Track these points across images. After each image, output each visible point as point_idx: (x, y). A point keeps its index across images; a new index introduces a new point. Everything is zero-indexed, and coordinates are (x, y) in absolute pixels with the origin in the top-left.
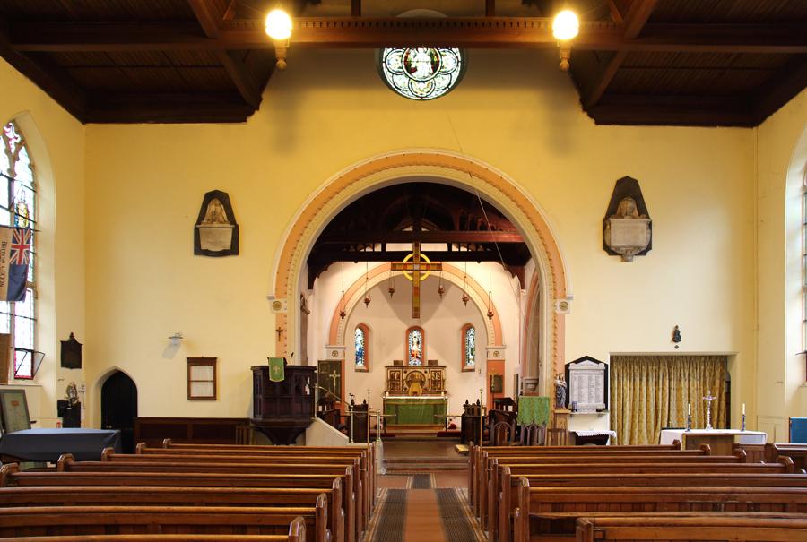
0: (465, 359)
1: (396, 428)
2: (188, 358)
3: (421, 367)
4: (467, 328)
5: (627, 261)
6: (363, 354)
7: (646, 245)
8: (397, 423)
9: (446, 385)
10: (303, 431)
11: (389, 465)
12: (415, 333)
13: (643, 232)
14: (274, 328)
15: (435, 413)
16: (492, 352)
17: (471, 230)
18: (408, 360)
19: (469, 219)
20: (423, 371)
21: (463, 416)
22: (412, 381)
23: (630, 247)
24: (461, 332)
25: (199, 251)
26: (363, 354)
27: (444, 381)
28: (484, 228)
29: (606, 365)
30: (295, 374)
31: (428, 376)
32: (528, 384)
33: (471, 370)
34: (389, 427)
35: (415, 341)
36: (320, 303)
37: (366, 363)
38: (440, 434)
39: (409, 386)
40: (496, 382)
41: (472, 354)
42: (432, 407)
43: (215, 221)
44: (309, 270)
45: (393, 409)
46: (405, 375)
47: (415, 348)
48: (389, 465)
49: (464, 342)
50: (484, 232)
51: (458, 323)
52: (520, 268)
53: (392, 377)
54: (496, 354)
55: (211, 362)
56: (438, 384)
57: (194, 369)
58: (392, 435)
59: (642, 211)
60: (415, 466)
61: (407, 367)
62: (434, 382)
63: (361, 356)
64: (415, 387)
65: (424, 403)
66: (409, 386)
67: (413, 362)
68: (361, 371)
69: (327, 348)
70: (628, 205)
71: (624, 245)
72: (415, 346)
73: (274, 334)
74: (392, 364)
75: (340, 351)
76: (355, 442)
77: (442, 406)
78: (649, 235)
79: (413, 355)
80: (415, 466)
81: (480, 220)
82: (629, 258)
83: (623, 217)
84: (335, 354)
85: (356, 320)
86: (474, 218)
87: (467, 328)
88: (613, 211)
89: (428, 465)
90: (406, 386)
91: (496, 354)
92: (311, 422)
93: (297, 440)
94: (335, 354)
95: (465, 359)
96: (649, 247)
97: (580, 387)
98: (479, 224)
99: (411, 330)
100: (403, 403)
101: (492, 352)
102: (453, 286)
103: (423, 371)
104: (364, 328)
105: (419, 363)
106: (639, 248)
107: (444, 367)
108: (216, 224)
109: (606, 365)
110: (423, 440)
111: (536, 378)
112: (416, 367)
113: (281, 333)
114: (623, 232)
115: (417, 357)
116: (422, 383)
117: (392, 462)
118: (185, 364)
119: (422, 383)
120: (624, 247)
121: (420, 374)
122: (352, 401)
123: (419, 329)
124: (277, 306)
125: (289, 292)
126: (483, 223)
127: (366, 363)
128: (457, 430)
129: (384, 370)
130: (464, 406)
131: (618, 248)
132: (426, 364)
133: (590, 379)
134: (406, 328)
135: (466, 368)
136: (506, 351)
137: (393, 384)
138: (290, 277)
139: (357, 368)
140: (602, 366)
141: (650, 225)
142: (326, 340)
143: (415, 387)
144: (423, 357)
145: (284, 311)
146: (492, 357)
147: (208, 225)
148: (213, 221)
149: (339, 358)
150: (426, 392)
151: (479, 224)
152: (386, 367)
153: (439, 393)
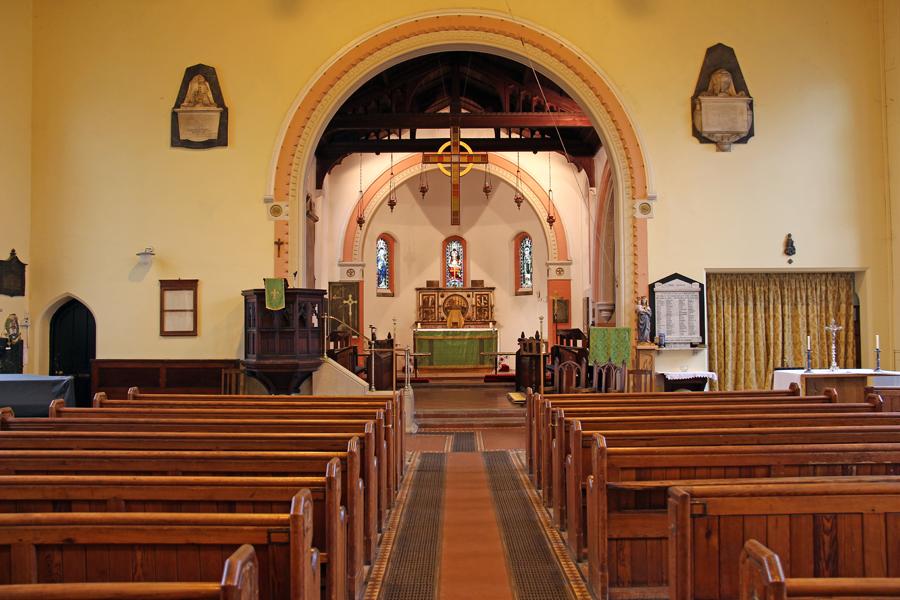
0: (519, 280)
1: (430, 371)
2: (161, 281)
3: (463, 290)
4: (522, 237)
5: (723, 151)
6: (387, 273)
7: (747, 130)
8: (431, 363)
9: (495, 313)
10: (309, 375)
11: (422, 421)
12: (455, 246)
13: (742, 113)
14: (272, 240)
15: (482, 349)
16: (553, 269)
17: (524, 111)
18: (445, 280)
19: (522, 98)
20: (464, 294)
21: (518, 355)
22: (451, 308)
23: (727, 132)
25: (177, 142)
26: (387, 273)
27: (492, 307)
28: (540, 108)
29: (701, 285)
30: (299, 299)
31: (472, 301)
32: (601, 311)
34: (422, 370)
35: (454, 255)
36: (332, 207)
37: (391, 286)
38: (488, 379)
40: (560, 308)
41: (528, 272)
42: (477, 343)
43: (198, 103)
44: (318, 163)
45: (426, 345)
46: (441, 301)
47: (454, 265)
48: (422, 421)
49: (518, 256)
50: (541, 114)
51: (510, 232)
52: (587, 159)
54: (560, 271)
55: (192, 285)
56: (485, 313)
57: (169, 295)
58: (426, 380)
59: (740, 87)
60: (455, 421)
61: (445, 290)
62: (480, 309)
63: (385, 275)
64: (455, 316)
65: (467, 337)
66: (447, 314)
67: (453, 282)
68: (384, 295)
69: (340, 265)
70: (723, 79)
71: (719, 130)
72: (455, 262)
73: (272, 248)
74: (425, 286)
75: (357, 270)
76: (377, 389)
77: (492, 338)
78: (750, 117)
79: (452, 274)
80: (455, 421)
81: (535, 98)
82: (726, 146)
83: (717, 95)
84: (351, 273)
85: (378, 228)
86: (527, 96)
87: (522, 237)
88: (703, 88)
89: (474, 421)
90: (443, 314)
91: (560, 271)
92: (320, 364)
93: (301, 388)
94: (351, 273)
95: (519, 280)
96: (751, 133)
97: (669, 315)
98: (534, 104)
99: (449, 240)
100: (440, 337)
101: (553, 269)
102: (502, 183)
103: (464, 294)
104: (388, 239)
105: (459, 284)
106: (738, 134)
107: (493, 289)
108: (199, 108)
109: (701, 285)
110: (466, 387)
111: (611, 302)
112: (455, 289)
113: (281, 246)
114: (718, 113)
115: (457, 277)
116: (464, 310)
117: (426, 416)
118: (157, 289)
119: (464, 310)
120: (720, 132)
122: (373, 335)
123: (459, 239)
124: (276, 211)
125: (291, 192)
126: (539, 102)
127: (391, 286)
128: (510, 373)
129: (415, 293)
130: (519, 340)
131: (712, 134)
132: (469, 285)
133: (681, 303)
134: (443, 238)
135: (520, 290)
136: (571, 267)
137: (426, 313)
138: (293, 173)
139: (379, 291)
140: (696, 287)
141: (751, 105)
142: (339, 255)
143: (455, 316)
144: (465, 274)
145: (287, 218)
146: (554, 276)
147: (189, 109)
148: (196, 103)
149: (355, 278)
150: (469, 322)
151: (534, 104)
152: (417, 289)
153: (486, 324)
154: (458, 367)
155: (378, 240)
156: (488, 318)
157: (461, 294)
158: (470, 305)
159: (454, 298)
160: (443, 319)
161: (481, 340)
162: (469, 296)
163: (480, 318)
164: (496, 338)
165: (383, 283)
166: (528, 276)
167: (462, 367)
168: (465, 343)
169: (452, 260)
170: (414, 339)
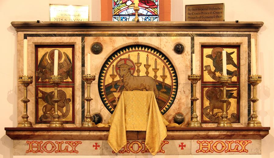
22: (121, 87)
27: (252, 83)
39: (111, 106)
66: (111, 106)
107: (254, 27)
121: (153, 58)
129: (11, 36)
156: (237, 118)
157: (154, 41)
158: (183, 79)
159: (133, 55)
160: (98, 119)
162: (179, 49)
163: (215, 119)
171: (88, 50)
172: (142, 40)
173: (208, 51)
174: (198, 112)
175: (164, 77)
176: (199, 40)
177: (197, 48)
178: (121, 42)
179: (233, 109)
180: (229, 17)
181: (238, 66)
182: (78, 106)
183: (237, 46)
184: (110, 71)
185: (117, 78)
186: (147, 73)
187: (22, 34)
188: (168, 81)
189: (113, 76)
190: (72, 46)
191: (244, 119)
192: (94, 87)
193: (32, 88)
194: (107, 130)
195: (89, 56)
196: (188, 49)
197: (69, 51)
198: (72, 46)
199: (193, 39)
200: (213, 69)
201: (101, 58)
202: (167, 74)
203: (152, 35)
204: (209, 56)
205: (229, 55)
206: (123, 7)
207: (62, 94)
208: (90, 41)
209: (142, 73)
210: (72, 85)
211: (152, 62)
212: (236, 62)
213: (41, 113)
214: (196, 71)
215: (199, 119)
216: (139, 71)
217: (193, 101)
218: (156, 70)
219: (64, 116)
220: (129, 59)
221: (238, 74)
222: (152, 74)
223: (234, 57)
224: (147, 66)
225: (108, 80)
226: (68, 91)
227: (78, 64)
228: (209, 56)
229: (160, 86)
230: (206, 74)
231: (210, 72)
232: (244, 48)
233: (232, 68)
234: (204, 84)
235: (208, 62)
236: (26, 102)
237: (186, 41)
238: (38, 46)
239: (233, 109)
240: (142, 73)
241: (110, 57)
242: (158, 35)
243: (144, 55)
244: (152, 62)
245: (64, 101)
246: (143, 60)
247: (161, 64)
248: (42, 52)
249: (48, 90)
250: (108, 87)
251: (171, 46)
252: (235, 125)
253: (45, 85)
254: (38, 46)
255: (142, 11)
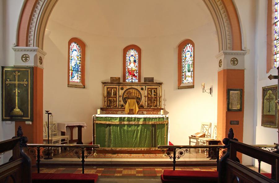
12: (132, 52)
20: (139, 88)
22: (128, 98)
24: (178, 49)
33: (192, 87)
35: (132, 59)
39: (125, 102)
46: (121, 92)
47: (132, 66)
53: (109, 93)
62: (150, 99)
74: (109, 81)
75: (32, 55)
90: (122, 103)
94: (25, 58)
100: (117, 122)
105: (136, 80)
107: (160, 84)
119: (138, 100)
129: (101, 85)
135: (182, 85)
143: (131, 104)
149: (31, 63)
154: (133, 149)
155: (70, 44)
156: (156, 106)
157: (136, 87)
159: (131, 90)
161: (154, 125)
162: (142, 89)
164: (167, 124)
165: (76, 77)
166: (189, 74)
167: (136, 149)
168: (140, 128)
169: (130, 63)
170: (94, 124)
171: (120, 89)
172: (133, 87)
173: (150, 89)
174: (146, 104)
175: (138, 96)
176: (147, 87)
177: (147, 89)
178: (128, 87)
179: (155, 104)
180: (155, 82)
181: (157, 93)
182: (117, 103)
183: (157, 88)
184: (125, 94)
185: (127, 96)
186: (134, 95)
187: (104, 85)
188: (139, 97)
189: (126, 95)
190: (116, 88)
191: (158, 106)
192: (122, 98)
193: (106, 98)
194: (125, 108)
195: (120, 91)
196: (144, 89)
197: (115, 89)
198: (116, 88)
199: (145, 87)
200: (150, 94)
201: (123, 91)
202: (139, 95)
203: (136, 86)
204: (150, 91)
205: (154, 91)
206: (129, 77)
207: (114, 100)
208: (120, 87)
209: (133, 95)
210: (116, 97)
211: (135, 92)
212: (156, 92)
213: (108, 104)
214: (146, 94)
215: (147, 106)
216: (132, 94)
217: (145, 102)
218: (136, 94)
219: (114, 105)
220: (130, 91)
221: (157, 95)
222: (135, 95)
223: (156, 91)
224: (134, 93)
225: (125, 96)
226: (115, 99)
227: (118, 92)
228: (150, 91)
229: (138, 98)
230: (149, 95)
231: (150, 95)
232: (158, 89)
233: (155, 94)
234: (148, 98)
235: (150, 92)
236: (105, 102)
237: (144, 87)
238: (108, 88)
239: (155, 104)
240: (133, 95)
241: (125, 91)
242: (137, 86)
243: (133, 90)
244: (135, 92)
245: (114, 101)
246: (133, 92)
247: (138, 93)
248: (109, 89)
249: (110, 99)
250: (125, 98)
251: (140, 88)
252: (155, 108)
253: (109, 97)
254: (108, 88)
255: (133, 78)
